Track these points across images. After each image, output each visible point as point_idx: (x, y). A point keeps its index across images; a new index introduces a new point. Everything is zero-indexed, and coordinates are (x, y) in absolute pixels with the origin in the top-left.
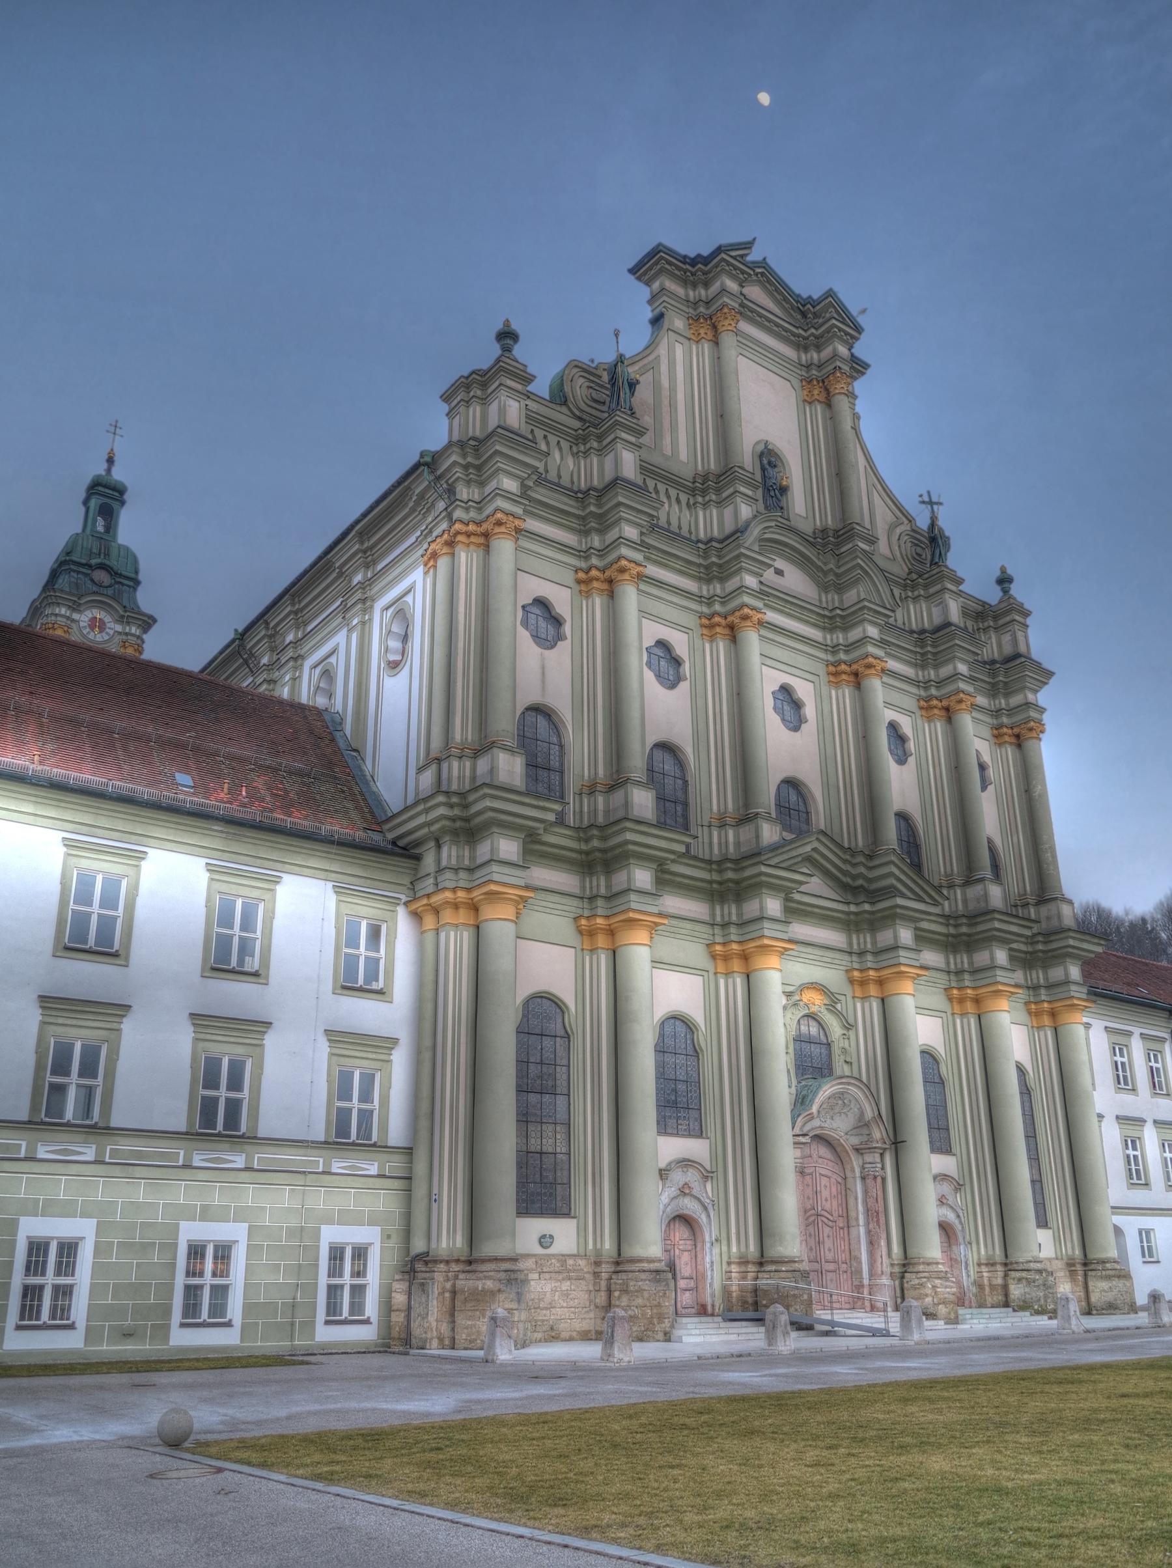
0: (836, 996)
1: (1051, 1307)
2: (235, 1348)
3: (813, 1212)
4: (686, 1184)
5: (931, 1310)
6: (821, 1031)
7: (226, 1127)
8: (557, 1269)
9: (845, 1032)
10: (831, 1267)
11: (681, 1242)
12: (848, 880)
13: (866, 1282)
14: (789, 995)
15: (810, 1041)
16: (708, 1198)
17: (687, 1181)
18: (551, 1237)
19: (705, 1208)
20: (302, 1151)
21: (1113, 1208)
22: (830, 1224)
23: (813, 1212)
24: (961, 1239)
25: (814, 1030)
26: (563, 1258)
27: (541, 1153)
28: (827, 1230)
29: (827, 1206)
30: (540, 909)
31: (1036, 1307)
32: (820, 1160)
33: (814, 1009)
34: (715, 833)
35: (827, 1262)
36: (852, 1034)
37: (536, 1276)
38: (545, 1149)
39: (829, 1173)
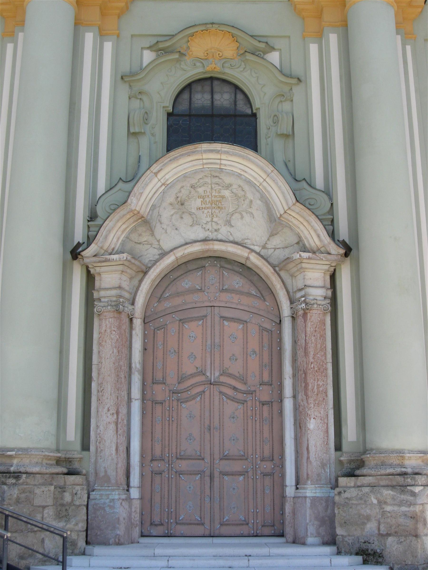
6: (240, 96)
9: (286, 89)
10: (237, 466)
13: (290, 491)
22: (240, 396)
32: (225, 297)
35: (225, 458)
36: (298, 91)
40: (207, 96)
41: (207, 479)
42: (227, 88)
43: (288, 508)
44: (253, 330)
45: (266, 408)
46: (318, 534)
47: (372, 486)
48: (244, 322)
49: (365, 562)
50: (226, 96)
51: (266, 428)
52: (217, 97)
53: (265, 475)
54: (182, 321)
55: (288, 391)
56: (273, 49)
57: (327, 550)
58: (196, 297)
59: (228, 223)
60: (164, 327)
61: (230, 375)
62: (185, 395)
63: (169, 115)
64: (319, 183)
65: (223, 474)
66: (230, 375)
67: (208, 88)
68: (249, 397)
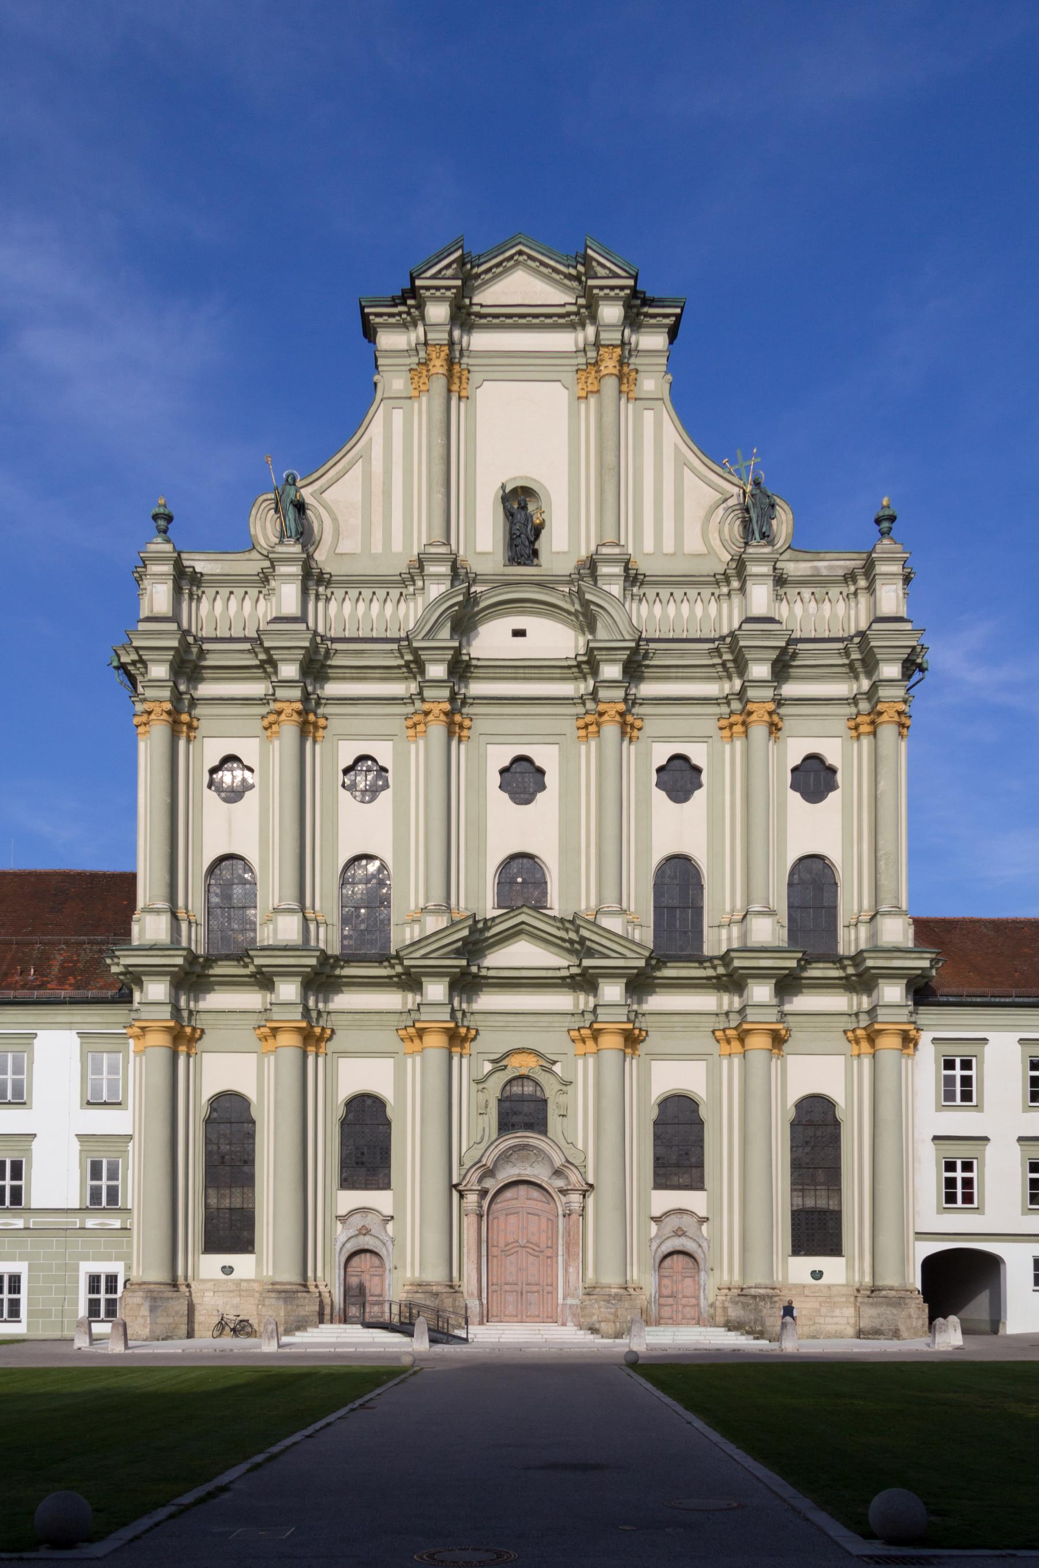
0: (547, 1055)
1: (759, 1328)
2: (24, 1334)
3: (517, 1244)
4: (364, 1226)
5: (597, 1326)
6: (538, 1088)
7: (12, 1203)
8: (231, 1289)
10: (535, 1288)
11: (371, 1269)
12: (567, 945)
13: (560, 1301)
14: (493, 1061)
15: (522, 1099)
16: (388, 1235)
17: (366, 1224)
18: (230, 1267)
19: (384, 1244)
20: (65, 1215)
21: (917, 1233)
22: (536, 1254)
23: (517, 1244)
24: (702, 1266)
25: (529, 1089)
26: (239, 1282)
27: (230, 1209)
28: (531, 1258)
29: (535, 1239)
30: (222, 1027)
31: (747, 1328)
32: (530, 1202)
33: (524, 1071)
34: (408, 930)
37: (211, 1294)
38: (233, 1206)
39: (539, 1213)
40: (520, 1088)
41: (520, 1295)
42: (531, 1083)
43: (559, 1309)
44: (544, 1220)
45: (549, 1260)
46: (572, 1321)
47: (596, 1300)
48: (538, 1215)
49: (592, 1333)
50: (531, 1089)
51: (549, 1269)
52: (526, 1089)
53: (548, 1293)
54: (507, 1215)
55: (560, 1252)
56: (554, 1062)
57: (576, 1328)
58: (514, 1202)
59: (531, 1166)
60: (497, 1218)
61: (531, 1243)
62: (508, 1253)
63: (499, 1100)
64: (580, 1146)
65: (527, 1292)
66: (531, 1243)
67: (520, 1083)
68: (541, 1254)
